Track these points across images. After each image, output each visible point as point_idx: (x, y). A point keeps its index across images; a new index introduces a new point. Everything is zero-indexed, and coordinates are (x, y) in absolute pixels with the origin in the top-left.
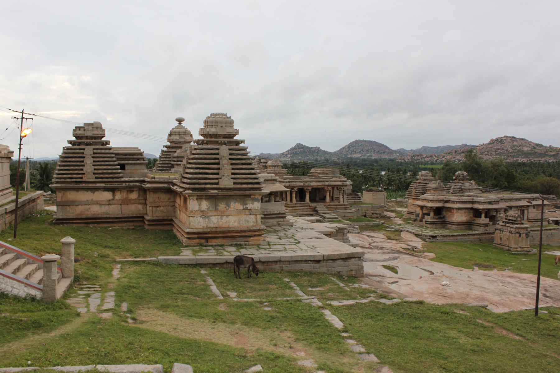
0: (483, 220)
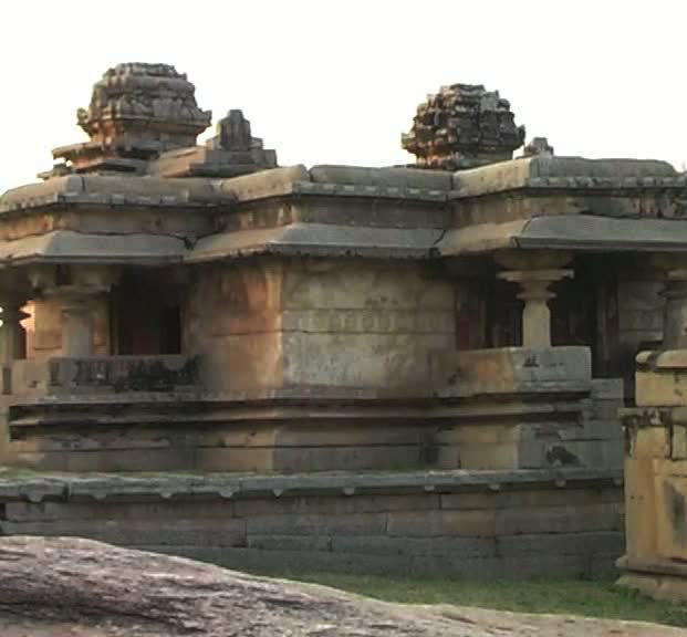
0: (537, 355)
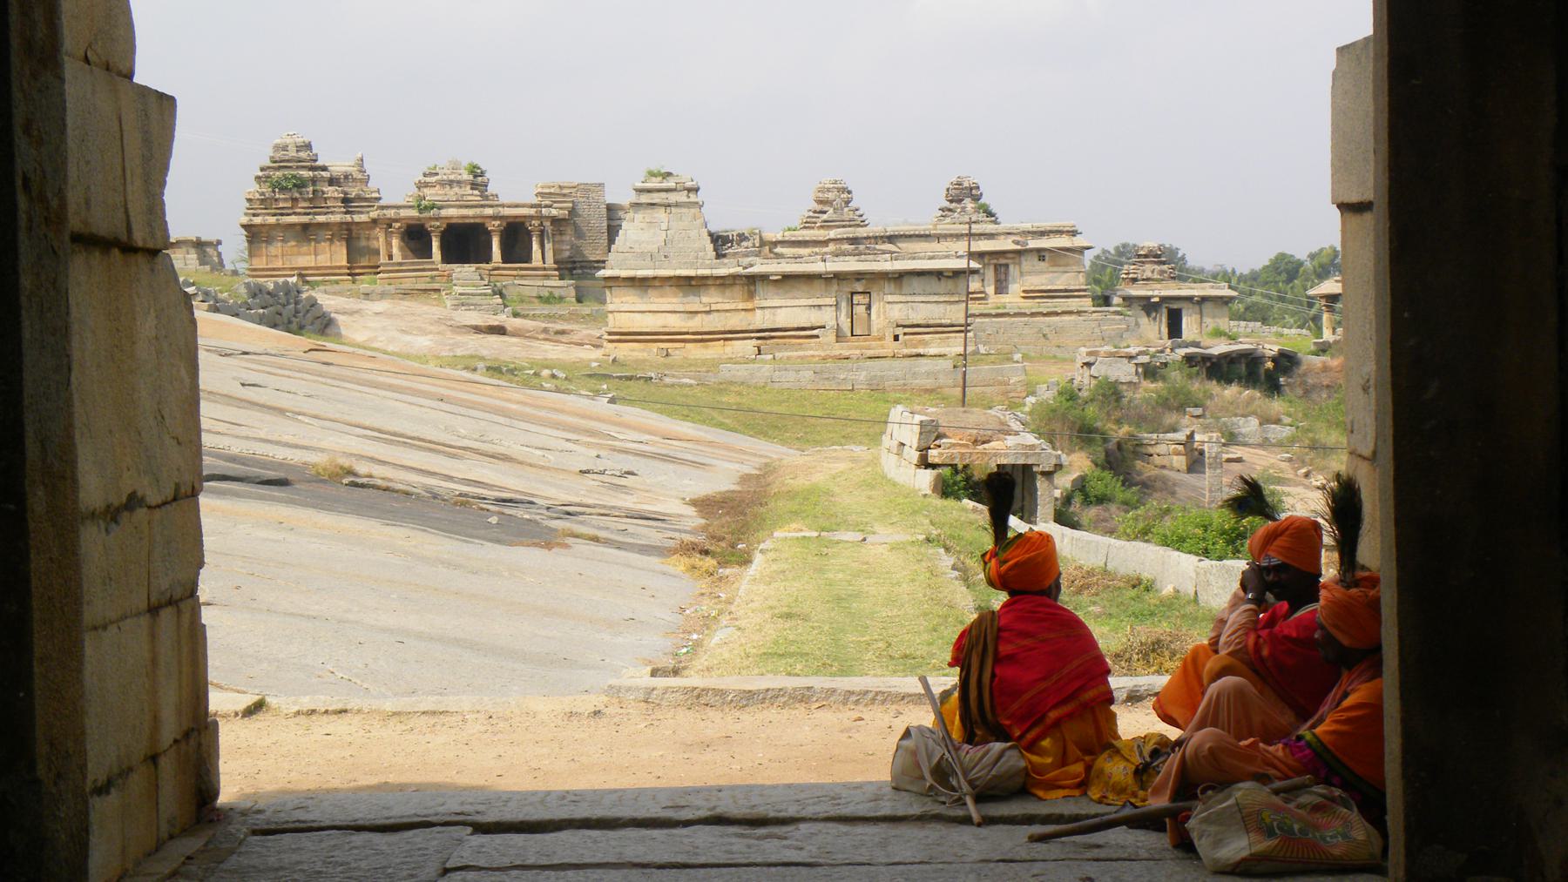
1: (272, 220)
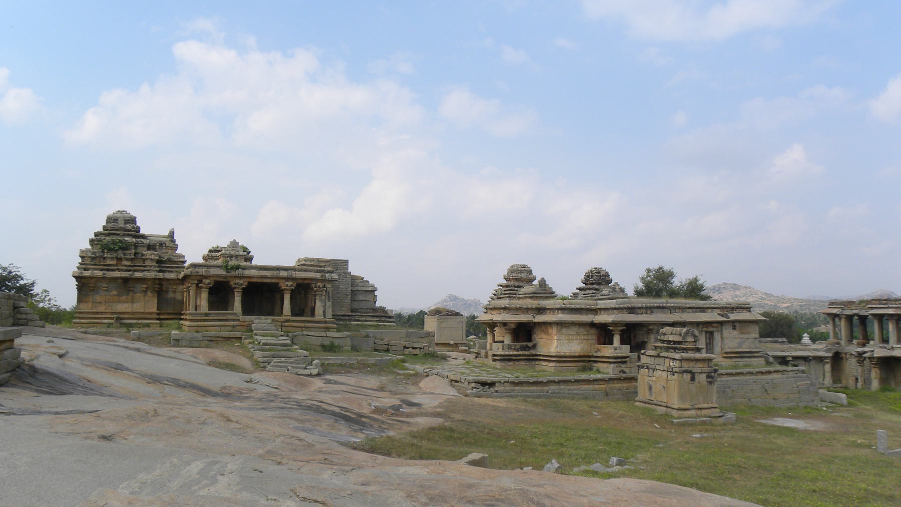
0: (617, 348)
1: (99, 274)
